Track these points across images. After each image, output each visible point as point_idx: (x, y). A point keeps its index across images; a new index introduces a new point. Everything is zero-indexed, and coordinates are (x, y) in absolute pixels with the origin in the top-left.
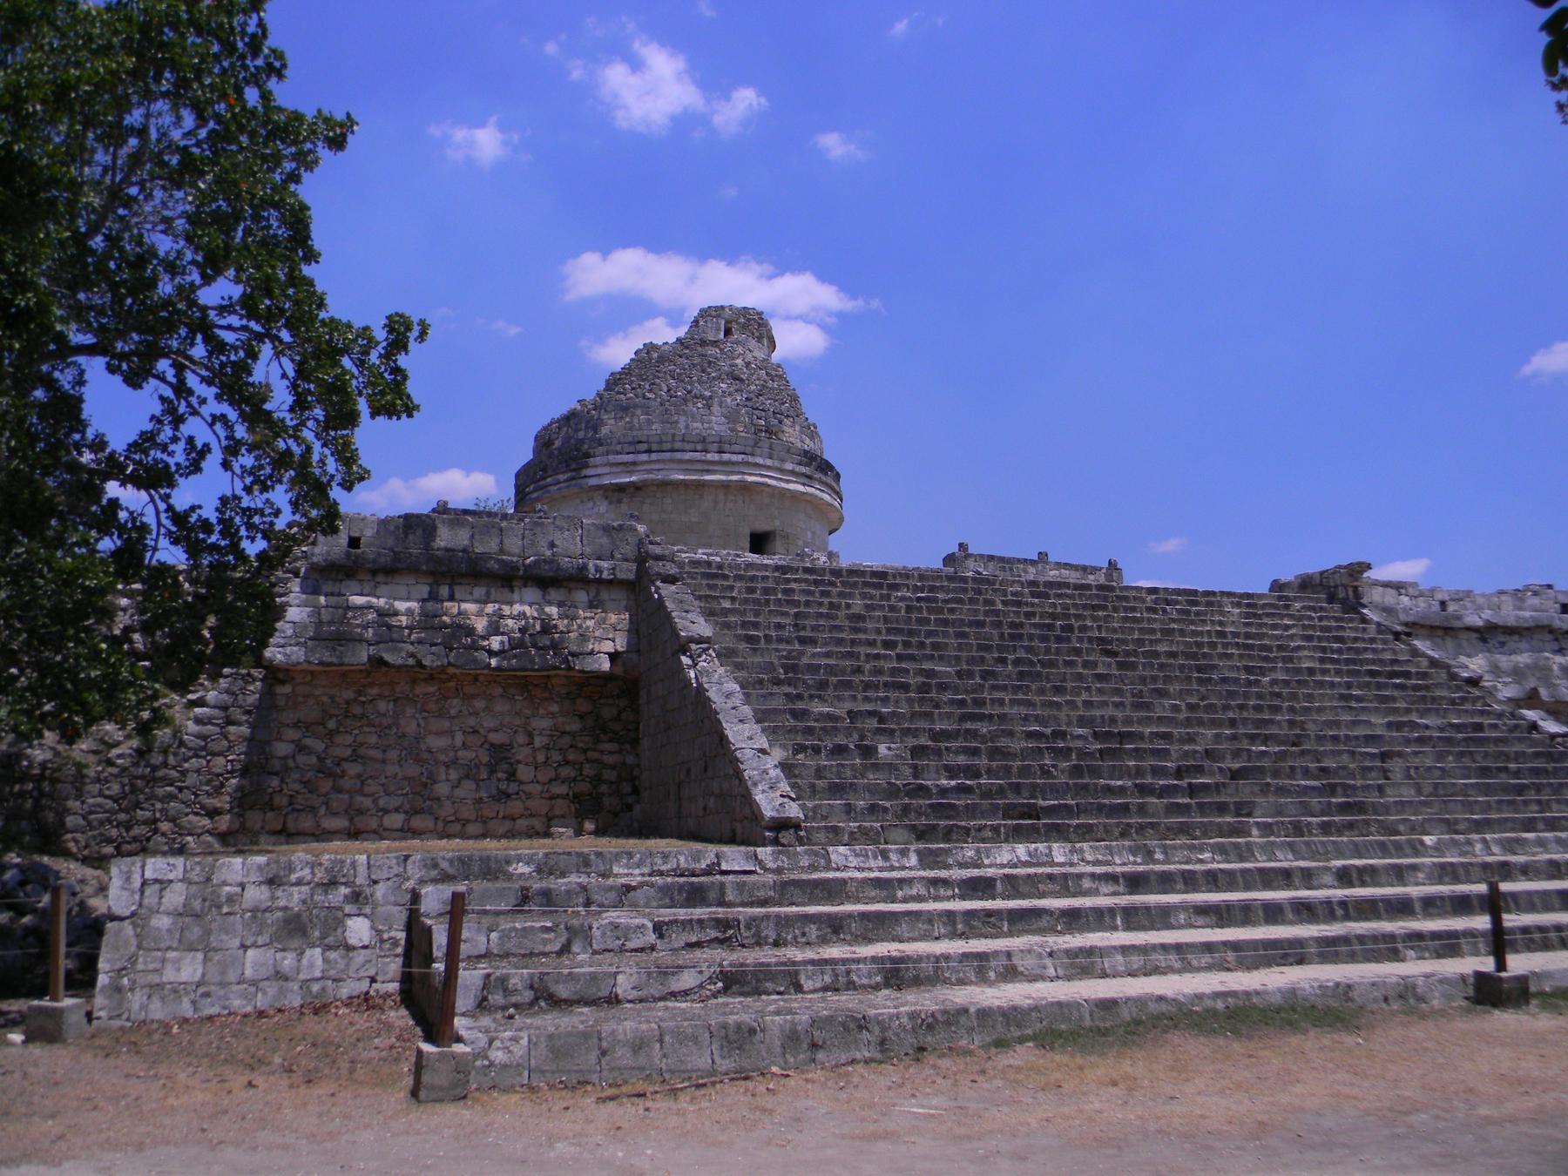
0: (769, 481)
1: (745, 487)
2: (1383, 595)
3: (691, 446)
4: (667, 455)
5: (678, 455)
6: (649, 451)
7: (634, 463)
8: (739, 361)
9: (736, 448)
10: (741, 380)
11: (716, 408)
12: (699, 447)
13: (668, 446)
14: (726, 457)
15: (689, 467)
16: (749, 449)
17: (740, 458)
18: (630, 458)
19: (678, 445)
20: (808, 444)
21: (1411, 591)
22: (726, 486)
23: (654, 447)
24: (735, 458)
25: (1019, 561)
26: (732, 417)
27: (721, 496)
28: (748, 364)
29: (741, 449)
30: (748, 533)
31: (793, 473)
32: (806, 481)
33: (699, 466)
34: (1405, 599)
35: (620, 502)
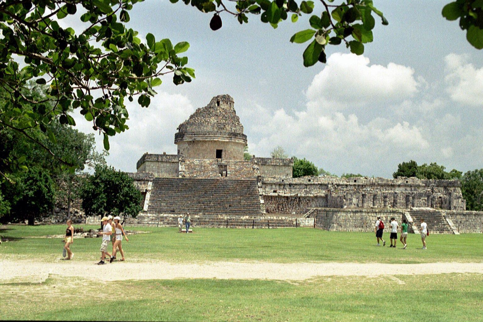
24: (212, 135)
34: (275, 180)
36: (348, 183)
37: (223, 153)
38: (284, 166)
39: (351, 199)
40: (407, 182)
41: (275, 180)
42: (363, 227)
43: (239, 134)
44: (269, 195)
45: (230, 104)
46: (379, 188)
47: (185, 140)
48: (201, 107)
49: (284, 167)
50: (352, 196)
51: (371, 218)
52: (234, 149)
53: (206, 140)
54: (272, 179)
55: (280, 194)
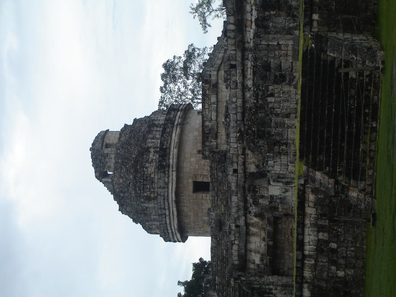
0: (174, 190)
2: (235, 250)
3: (164, 219)
4: (168, 226)
5: (168, 222)
6: (167, 229)
7: (172, 232)
8: (121, 181)
10: (130, 183)
12: (164, 216)
13: (165, 225)
15: (172, 219)
16: (162, 198)
17: (166, 203)
18: (171, 235)
19: (163, 222)
20: (153, 156)
21: (233, 239)
22: (178, 202)
23: (165, 228)
25: (203, 130)
26: (149, 199)
27: (183, 204)
28: (122, 178)
29: (162, 201)
30: (195, 195)
31: (168, 177)
32: (171, 169)
33: (172, 216)
35: (187, 231)
36: (239, 86)
37: (200, 179)
38: (217, 94)
41: (236, 242)
45: (107, 146)
47: (180, 240)
48: (117, 206)
50: (262, 197)
53: (175, 213)
54: (235, 247)
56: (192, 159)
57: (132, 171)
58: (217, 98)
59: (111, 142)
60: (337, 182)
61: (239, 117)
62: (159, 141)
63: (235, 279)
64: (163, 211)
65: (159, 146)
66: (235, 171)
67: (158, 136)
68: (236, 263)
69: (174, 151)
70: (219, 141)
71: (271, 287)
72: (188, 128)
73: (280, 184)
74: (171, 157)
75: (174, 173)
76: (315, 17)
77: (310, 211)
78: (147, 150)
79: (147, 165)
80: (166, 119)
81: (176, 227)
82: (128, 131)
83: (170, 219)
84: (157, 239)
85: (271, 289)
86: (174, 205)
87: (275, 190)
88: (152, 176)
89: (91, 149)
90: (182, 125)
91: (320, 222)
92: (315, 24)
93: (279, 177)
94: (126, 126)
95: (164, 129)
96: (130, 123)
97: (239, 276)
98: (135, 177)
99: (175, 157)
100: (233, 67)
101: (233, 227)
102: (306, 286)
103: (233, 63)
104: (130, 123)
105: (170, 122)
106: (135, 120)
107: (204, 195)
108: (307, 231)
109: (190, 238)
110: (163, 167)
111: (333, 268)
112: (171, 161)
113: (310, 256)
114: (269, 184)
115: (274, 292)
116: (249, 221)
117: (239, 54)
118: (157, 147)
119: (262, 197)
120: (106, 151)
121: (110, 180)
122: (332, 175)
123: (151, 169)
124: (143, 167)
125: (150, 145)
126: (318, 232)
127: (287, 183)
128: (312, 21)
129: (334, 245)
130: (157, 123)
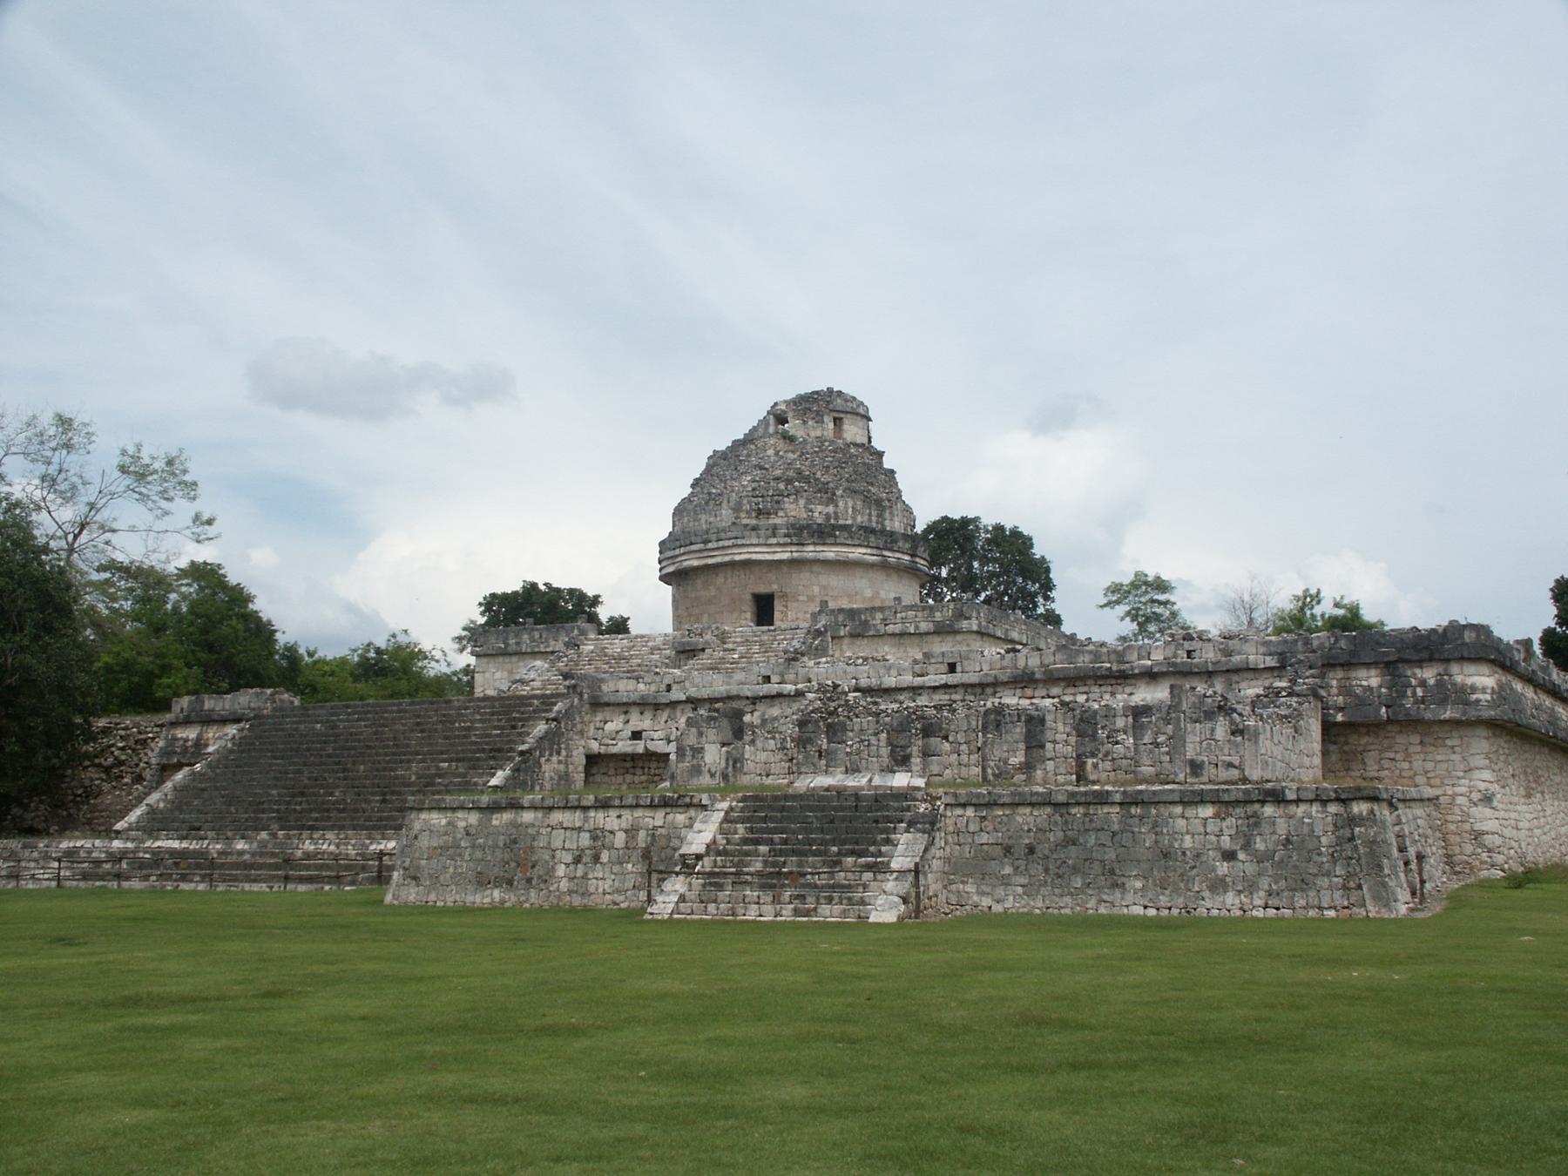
0: (754, 557)
1: (747, 564)
5: (693, 547)
9: (730, 534)
11: (725, 505)
14: (721, 544)
17: (730, 543)
20: (820, 512)
22: (732, 565)
24: (727, 543)
26: (737, 509)
28: (777, 453)
30: (748, 597)
31: (778, 544)
32: (794, 548)
34: (641, 686)
36: (918, 681)
39: (698, 751)
40: (1189, 653)
41: (641, 686)
42: (510, 883)
43: (845, 528)
44: (614, 750)
46: (1055, 691)
49: (937, 639)
50: (701, 734)
51: (558, 839)
52: (824, 588)
53: (710, 561)
54: (631, 685)
55: (652, 746)
56: (816, 589)
57: (791, 473)
58: (928, 634)
59: (845, 427)
60: (699, 857)
61: (864, 682)
62: (849, 522)
63: (574, 687)
64: (714, 537)
65: (841, 522)
66: (767, 679)
67: (859, 519)
68: (605, 688)
69: (830, 553)
70: (846, 641)
71: (564, 753)
72: (879, 576)
73: (723, 764)
74: (819, 548)
75: (785, 556)
76: (970, 812)
77: (659, 818)
78: (832, 500)
79: (802, 502)
80: (892, 534)
81: (686, 564)
82: (868, 459)
83: (700, 551)
84: (664, 529)
85: (559, 753)
86: (727, 559)
87: (713, 755)
88: (781, 513)
89: (830, 390)
90: (884, 566)
91: (642, 834)
92: (959, 811)
93: (735, 762)
94: (881, 454)
95: (873, 531)
96: (887, 463)
97: (581, 694)
98: (777, 479)
99: (821, 556)
100: (952, 668)
101: (666, 681)
102: (540, 815)
103: (959, 668)
104: (887, 463)
105: (889, 539)
106: (892, 472)
107: (749, 615)
108: (627, 814)
109: (668, 590)
110: (802, 532)
111: (569, 858)
112: (811, 548)
113: (586, 820)
114: (724, 745)
115: (555, 759)
116: (680, 707)
117: (972, 678)
118: (837, 518)
119: (701, 734)
120: (826, 419)
121: (771, 430)
122: (711, 848)
123: (795, 509)
124: (797, 492)
125: (841, 503)
126: (626, 831)
127: (725, 776)
128: (964, 806)
129: (605, 856)
130: (887, 515)
